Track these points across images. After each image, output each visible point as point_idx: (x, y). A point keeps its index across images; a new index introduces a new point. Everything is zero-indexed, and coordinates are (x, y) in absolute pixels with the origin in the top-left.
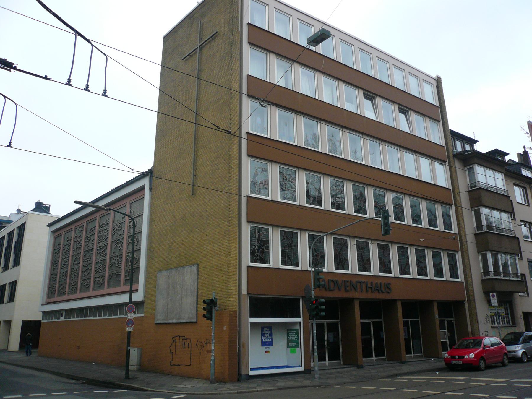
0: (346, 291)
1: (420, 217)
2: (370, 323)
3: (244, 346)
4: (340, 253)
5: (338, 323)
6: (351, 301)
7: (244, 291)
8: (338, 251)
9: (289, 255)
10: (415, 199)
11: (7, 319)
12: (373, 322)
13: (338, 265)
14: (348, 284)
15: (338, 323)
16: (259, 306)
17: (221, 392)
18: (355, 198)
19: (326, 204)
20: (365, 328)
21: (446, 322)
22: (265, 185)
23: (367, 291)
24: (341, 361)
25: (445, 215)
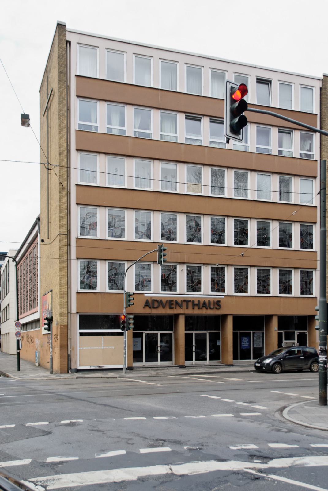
0: (170, 308)
1: (268, 238)
2: (206, 333)
3: (73, 349)
4: (168, 277)
5: (172, 334)
6: (177, 316)
7: (74, 309)
8: (166, 276)
9: (115, 280)
10: (143, 214)
11: (8, 332)
12: (209, 333)
13: (165, 288)
14: (174, 303)
15: (172, 334)
16: (87, 321)
17: (61, 378)
18: (189, 228)
19: (130, 235)
20: (188, 337)
21: (239, 333)
22: (93, 226)
23: (193, 308)
24: (221, 361)
25: (304, 234)
